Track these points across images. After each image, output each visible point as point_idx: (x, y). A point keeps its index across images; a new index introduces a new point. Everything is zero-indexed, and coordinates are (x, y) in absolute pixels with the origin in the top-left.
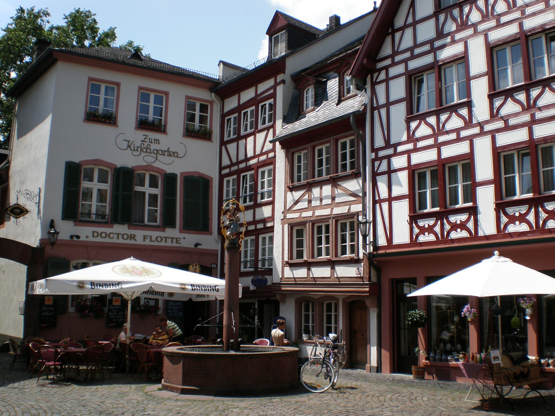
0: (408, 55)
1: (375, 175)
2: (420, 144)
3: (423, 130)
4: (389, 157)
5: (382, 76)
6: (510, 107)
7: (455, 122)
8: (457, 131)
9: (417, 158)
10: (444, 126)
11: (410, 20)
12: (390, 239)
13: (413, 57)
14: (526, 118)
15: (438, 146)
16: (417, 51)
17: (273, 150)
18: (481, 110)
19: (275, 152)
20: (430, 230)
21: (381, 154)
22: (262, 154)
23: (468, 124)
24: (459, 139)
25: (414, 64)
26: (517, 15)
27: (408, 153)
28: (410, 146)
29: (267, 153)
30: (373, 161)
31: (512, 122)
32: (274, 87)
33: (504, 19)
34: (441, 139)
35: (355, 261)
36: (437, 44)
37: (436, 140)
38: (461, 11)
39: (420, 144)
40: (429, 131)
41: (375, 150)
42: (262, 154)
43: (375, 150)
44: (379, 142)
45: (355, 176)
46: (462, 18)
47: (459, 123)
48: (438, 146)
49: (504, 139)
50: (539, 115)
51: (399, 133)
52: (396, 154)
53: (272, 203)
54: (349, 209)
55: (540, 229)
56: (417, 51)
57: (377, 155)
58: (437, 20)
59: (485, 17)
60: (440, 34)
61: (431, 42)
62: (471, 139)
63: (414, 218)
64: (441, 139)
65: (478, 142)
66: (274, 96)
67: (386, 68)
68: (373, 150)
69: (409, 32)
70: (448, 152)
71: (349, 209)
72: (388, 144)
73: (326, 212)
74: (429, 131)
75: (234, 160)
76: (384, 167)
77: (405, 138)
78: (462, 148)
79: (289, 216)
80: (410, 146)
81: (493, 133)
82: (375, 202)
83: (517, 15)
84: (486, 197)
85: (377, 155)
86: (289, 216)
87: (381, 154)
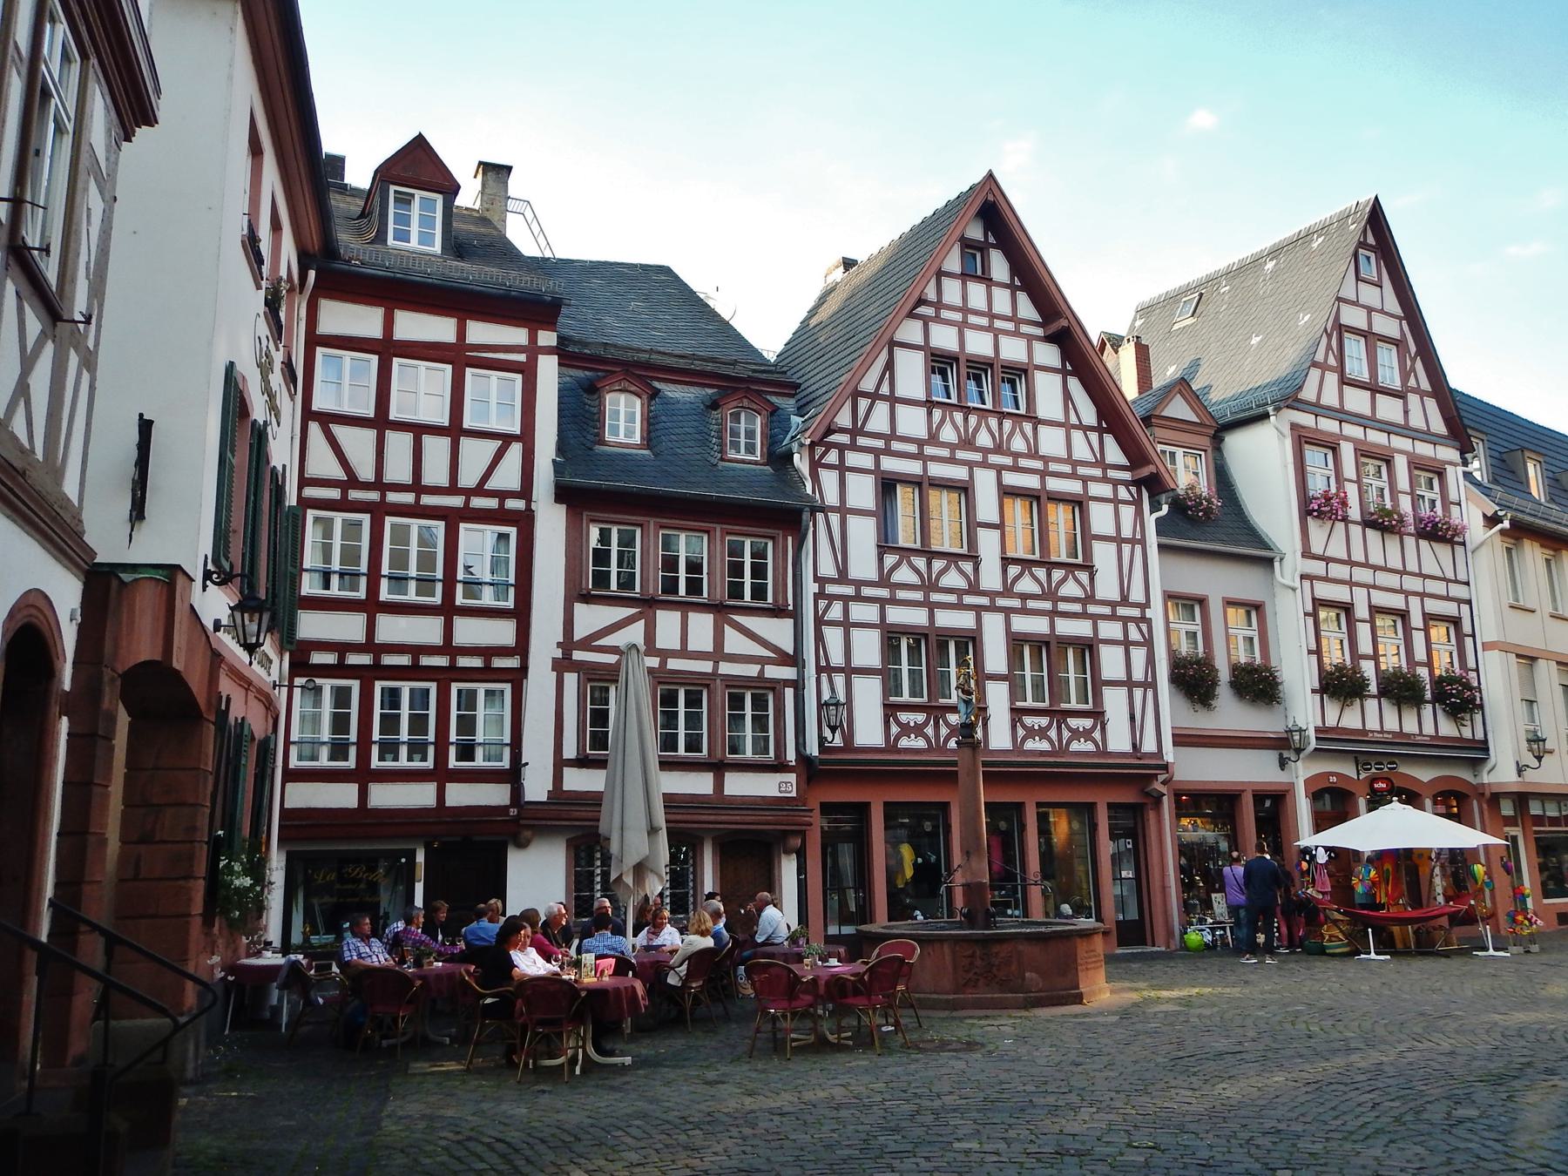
0: (880, 444)
1: (820, 622)
2: (902, 595)
3: (904, 575)
4: (845, 599)
5: (832, 457)
6: (1026, 585)
7: (953, 579)
8: (960, 593)
9: (896, 615)
10: (938, 578)
11: (885, 390)
12: (849, 737)
13: (888, 452)
14: (1047, 605)
15: (932, 607)
16: (896, 446)
17: (526, 492)
18: (991, 578)
19: (529, 501)
20: (918, 730)
21: (831, 589)
22: (480, 490)
23: (974, 589)
24: (959, 606)
25: (888, 464)
26: (1038, 465)
27: (882, 602)
28: (884, 593)
29: (502, 495)
30: (817, 597)
31: (1031, 604)
32: (533, 350)
33: (1023, 463)
34: (935, 597)
35: (779, 767)
36: (929, 450)
37: (927, 596)
38: (966, 420)
39: (902, 595)
40: (913, 579)
41: (821, 581)
42: (480, 490)
43: (821, 581)
44: (828, 568)
45: (777, 612)
46: (966, 430)
47: (962, 583)
48: (932, 607)
49: (1022, 624)
50: (1062, 606)
51: (863, 564)
52: (858, 598)
53: (521, 614)
54: (762, 671)
55: (1062, 749)
56: (896, 446)
57: (822, 588)
58: (930, 414)
59: (999, 449)
60: (933, 439)
61: (920, 443)
62: (979, 609)
63: (890, 710)
64: (935, 597)
65: (987, 618)
66: (529, 373)
67: (842, 448)
68: (816, 579)
69: (882, 408)
70: (945, 619)
71: (762, 671)
72: (843, 577)
73: (706, 667)
74: (913, 579)
75: (366, 473)
76: (836, 612)
77: (873, 575)
78: (965, 620)
79: (578, 655)
80: (884, 593)
81: (1008, 611)
82: (819, 670)
83: (1038, 465)
84: (997, 697)
85: (822, 588)
86: (578, 655)
87: (831, 589)
